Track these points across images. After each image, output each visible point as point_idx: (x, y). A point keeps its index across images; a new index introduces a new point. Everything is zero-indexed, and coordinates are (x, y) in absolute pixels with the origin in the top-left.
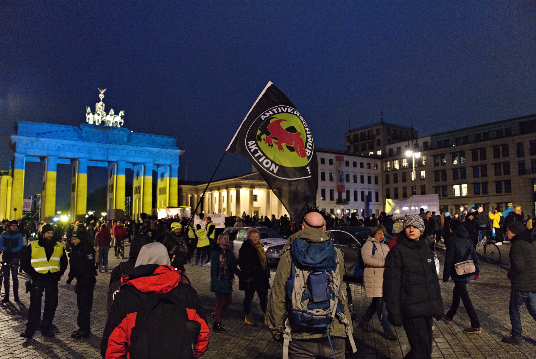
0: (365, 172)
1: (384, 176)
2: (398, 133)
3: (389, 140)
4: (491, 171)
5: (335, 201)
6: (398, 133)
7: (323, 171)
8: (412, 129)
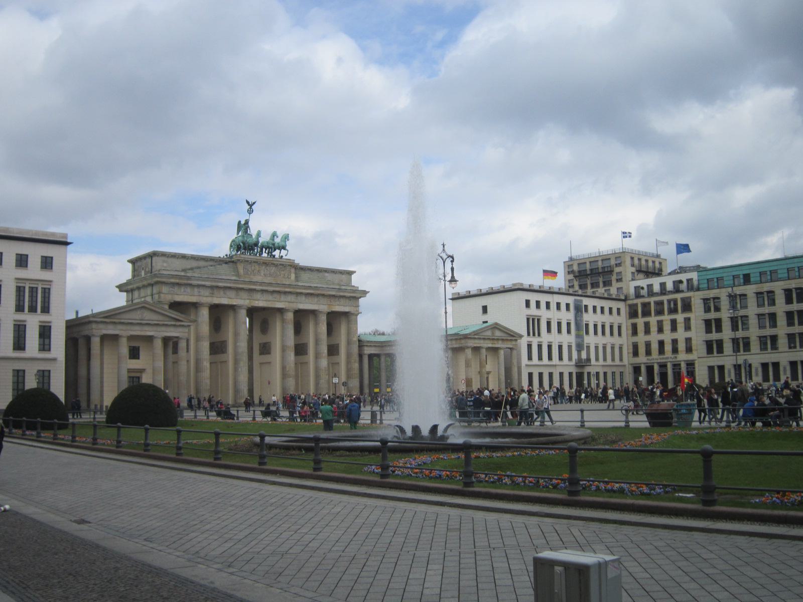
0: (607, 319)
1: (629, 324)
2: (643, 262)
3: (633, 273)
4: (782, 321)
5: (573, 363)
6: (643, 262)
7: (587, 323)
8: (658, 256)
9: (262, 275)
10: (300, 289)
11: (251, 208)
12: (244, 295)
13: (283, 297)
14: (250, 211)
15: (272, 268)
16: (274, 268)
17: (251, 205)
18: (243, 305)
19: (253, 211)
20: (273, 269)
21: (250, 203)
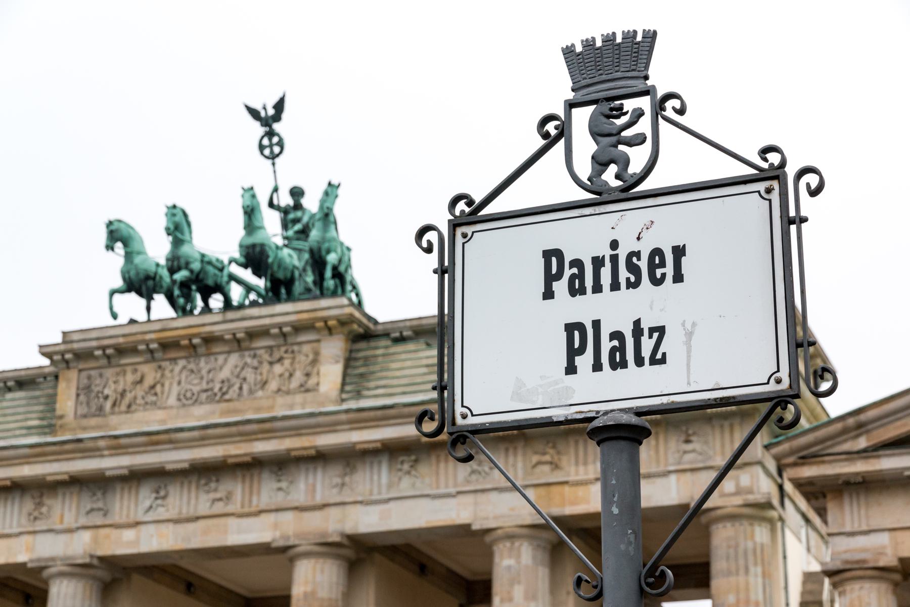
9: (172, 401)
10: (332, 427)
11: (271, 134)
12: (65, 510)
13: (268, 491)
14: (271, 146)
15: (221, 358)
16: (234, 359)
17: (269, 119)
18: (53, 559)
19: (281, 144)
20: (228, 365)
21: (263, 114)
